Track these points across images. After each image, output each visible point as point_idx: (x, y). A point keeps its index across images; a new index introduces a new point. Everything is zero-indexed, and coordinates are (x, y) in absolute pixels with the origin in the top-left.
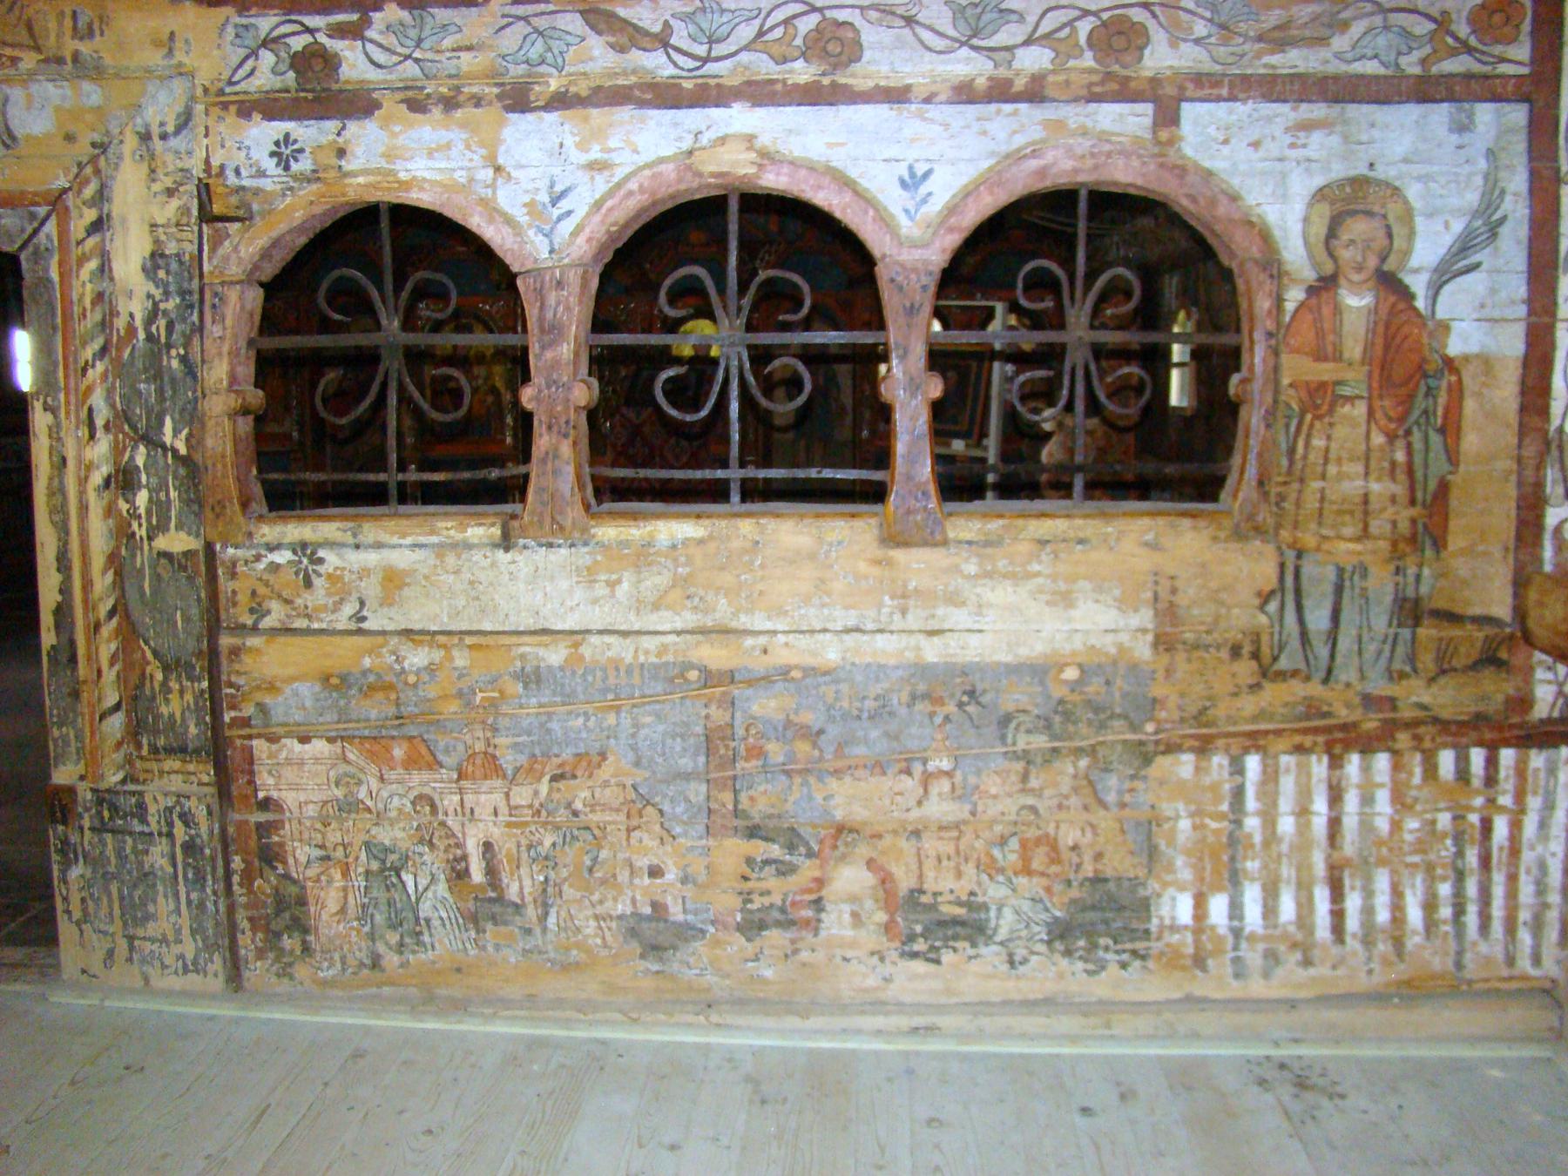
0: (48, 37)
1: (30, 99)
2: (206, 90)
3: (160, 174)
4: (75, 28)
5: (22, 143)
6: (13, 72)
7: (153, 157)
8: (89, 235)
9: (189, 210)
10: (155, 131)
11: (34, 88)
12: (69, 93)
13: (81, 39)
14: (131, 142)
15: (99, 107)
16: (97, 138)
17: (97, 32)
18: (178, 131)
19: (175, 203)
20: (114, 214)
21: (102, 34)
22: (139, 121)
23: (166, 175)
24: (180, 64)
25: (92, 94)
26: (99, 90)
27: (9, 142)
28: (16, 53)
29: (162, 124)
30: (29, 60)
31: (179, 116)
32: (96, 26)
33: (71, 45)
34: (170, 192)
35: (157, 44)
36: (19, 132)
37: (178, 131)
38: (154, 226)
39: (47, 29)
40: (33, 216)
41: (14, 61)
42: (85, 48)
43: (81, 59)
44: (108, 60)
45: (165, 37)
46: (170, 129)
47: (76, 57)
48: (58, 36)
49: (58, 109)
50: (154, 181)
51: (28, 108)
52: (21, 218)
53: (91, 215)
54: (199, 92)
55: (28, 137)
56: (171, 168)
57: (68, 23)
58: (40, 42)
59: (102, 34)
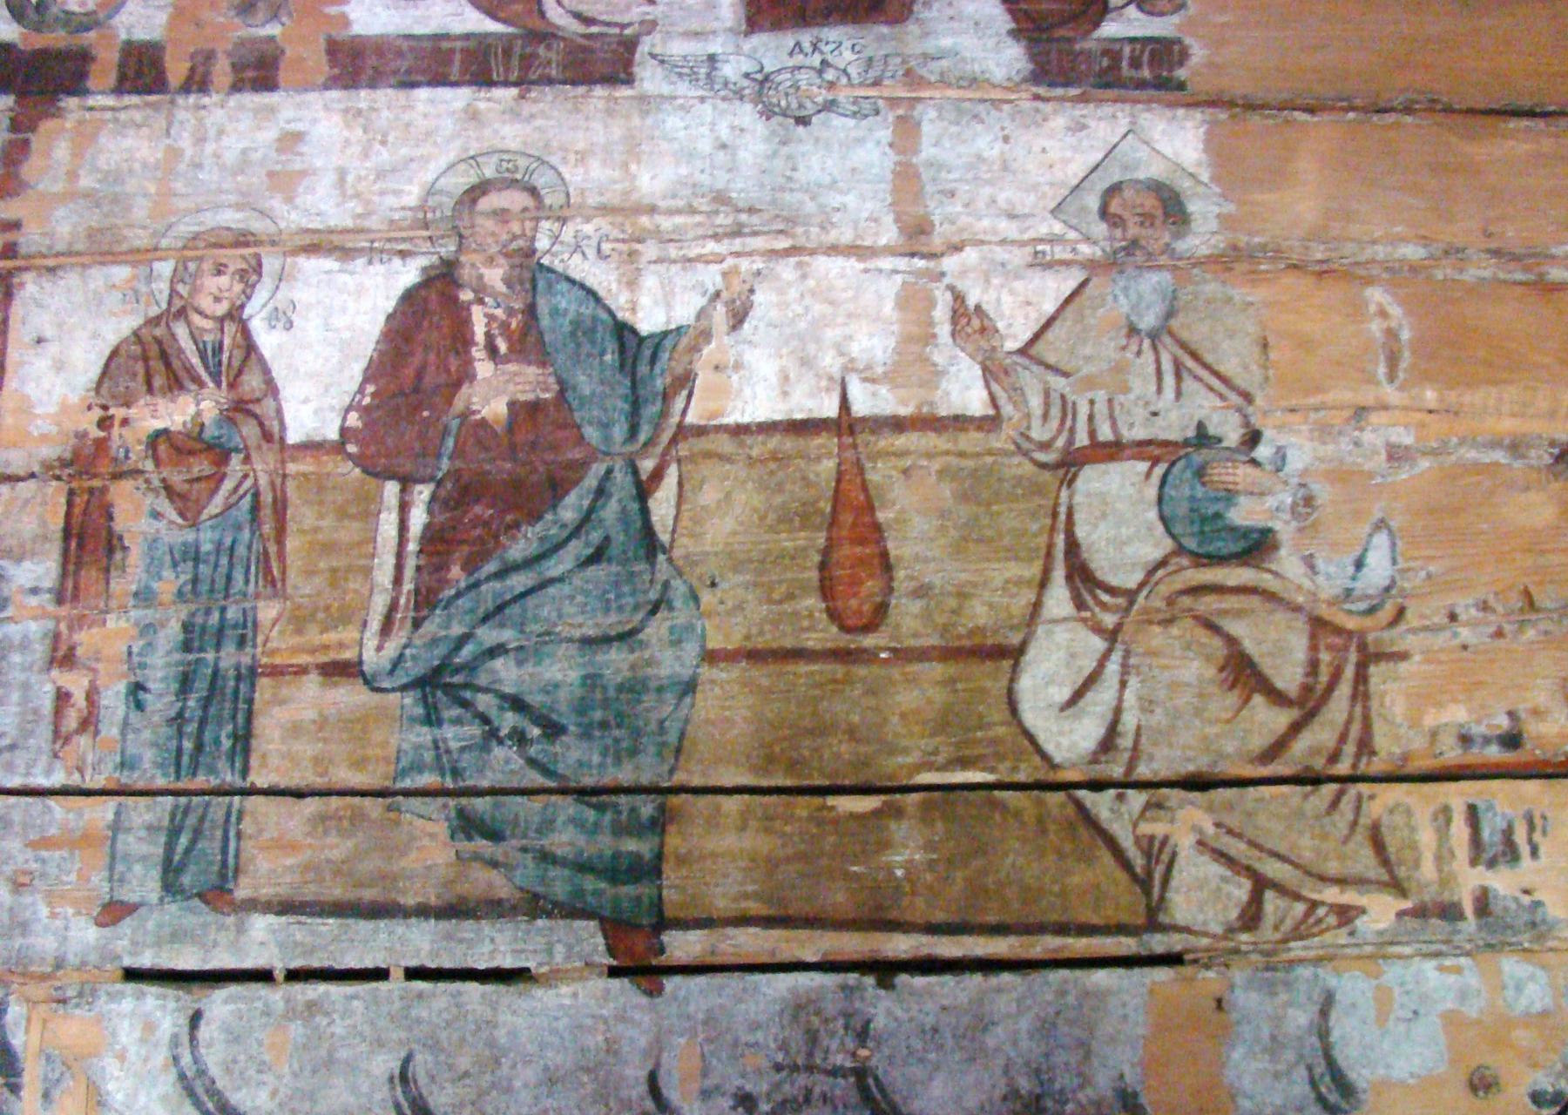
0: (1417, 864)
1: (1383, 999)
4: (1476, 842)
5: (1367, 1097)
6: (1342, 937)
11: (1393, 973)
12: (1472, 979)
13: (1492, 864)
15: (1544, 1013)
17: (1525, 850)
21: (1534, 852)
25: (1527, 984)
27: (1333, 1098)
28: (1350, 897)
30: (1380, 912)
32: (1520, 837)
33: (1469, 880)
36: (1359, 1076)
39: (1414, 846)
41: (1346, 915)
42: (1502, 882)
43: (1496, 907)
47: (1483, 903)
49: (1453, 1022)
51: (1382, 1017)
55: (1385, 1084)
57: (1460, 830)
58: (1402, 872)
59: (1534, 852)
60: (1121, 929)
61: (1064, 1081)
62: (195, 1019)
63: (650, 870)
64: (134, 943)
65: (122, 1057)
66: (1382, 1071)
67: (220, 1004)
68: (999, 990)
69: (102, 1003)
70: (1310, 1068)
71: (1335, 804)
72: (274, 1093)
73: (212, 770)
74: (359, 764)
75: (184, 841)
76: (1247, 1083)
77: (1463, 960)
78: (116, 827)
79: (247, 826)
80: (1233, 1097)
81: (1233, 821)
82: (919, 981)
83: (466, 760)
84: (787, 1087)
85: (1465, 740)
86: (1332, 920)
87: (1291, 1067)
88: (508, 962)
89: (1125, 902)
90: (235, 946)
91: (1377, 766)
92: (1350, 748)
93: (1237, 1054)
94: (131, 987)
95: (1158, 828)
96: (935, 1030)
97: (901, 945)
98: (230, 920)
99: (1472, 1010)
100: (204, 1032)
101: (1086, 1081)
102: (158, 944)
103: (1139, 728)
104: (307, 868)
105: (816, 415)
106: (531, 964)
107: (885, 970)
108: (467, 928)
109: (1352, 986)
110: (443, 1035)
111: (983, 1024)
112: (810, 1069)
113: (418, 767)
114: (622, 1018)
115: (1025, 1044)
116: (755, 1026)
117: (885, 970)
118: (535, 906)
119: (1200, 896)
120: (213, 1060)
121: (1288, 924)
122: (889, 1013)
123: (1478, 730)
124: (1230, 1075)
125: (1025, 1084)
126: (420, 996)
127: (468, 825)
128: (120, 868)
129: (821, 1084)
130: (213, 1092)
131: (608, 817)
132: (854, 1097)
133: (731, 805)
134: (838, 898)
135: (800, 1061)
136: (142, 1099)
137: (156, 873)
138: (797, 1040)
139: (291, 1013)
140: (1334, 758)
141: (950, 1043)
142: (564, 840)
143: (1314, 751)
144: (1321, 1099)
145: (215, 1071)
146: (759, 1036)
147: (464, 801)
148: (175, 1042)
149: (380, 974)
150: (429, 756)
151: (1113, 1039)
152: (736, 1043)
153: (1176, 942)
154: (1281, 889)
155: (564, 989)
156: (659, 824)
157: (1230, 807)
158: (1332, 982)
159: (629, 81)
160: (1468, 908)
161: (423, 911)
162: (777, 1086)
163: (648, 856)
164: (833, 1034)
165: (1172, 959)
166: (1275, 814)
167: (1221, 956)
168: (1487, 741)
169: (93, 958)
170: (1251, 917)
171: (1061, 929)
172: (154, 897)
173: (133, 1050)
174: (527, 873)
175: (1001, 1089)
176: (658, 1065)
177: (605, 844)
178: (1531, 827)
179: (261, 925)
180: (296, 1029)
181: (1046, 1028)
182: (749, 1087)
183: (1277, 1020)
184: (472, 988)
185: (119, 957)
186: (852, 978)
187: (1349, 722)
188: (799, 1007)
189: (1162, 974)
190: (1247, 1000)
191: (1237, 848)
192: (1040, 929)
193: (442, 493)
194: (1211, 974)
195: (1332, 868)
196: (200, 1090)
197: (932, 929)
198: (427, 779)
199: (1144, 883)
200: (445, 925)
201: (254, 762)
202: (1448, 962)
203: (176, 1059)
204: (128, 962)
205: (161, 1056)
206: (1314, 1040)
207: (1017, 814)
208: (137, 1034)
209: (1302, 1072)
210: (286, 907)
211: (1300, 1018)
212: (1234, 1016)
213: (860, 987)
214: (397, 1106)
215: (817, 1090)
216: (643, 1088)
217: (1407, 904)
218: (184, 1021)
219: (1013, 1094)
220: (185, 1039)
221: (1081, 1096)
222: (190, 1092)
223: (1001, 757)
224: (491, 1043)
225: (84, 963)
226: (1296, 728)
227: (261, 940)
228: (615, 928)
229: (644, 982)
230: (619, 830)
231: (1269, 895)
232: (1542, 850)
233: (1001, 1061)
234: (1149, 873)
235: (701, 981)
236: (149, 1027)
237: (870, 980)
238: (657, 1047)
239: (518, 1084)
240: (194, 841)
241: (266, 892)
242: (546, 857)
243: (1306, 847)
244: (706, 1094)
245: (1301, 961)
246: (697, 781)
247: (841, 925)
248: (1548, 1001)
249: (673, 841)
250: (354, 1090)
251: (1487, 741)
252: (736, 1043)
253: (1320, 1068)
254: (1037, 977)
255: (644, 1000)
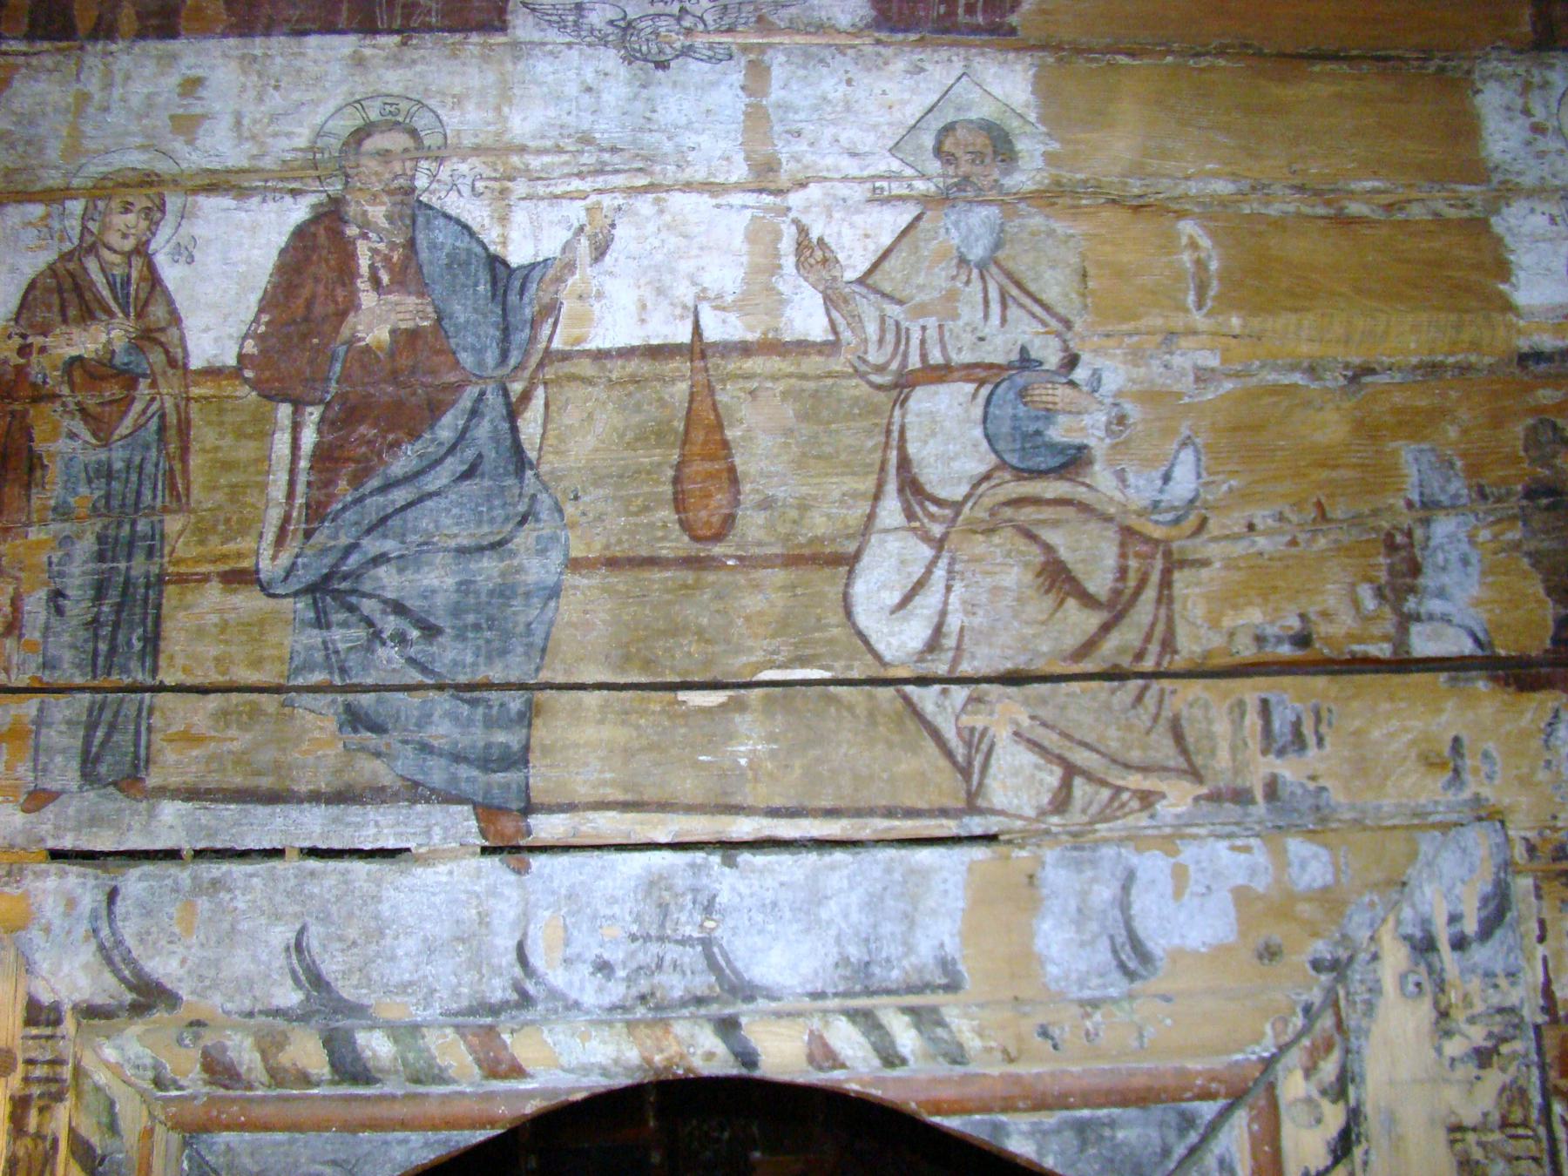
0: (1213, 752)
1: (1180, 875)
2: (1531, 849)
3: (1459, 1016)
5: (1163, 965)
6: (1143, 820)
7: (1441, 986)
8: (1336, 1161)
9: (1523, 1092)
10: (1443, 938)
11: (1188, 853)
12: (1260, 857)
13: (1281, 753)
14: (1395, 957)
15: (1325, 889)
16: (1321, 948)
17: (1311, 740)
18: (1485, 933)
19: (1494, 1079)
20: (1368, 1109)
21: (1320, 742)
22: (1407, 913)
23: (1472, 1020)
24: (1477, 800)
26: (1324, 855)
27: (1132, 964)
29: (1454, 919)
30: (1177, 799)
31: (1485, 901)
32: (1307, 730)
33: (1263, 767)
34: (1483, 1057)
35: (1431, 762)
36: (1157, 945)
37: (1485, 933)
38: (1457, 1128)
39: (1210, 736)
40: (1187, 1121)
41: (1147, 799)
42: (1288, 770)
43: (1284, 793)
44: (1337, 795)
45: (1446, 750)
46: (1470, 927)
47: (1272, 789)
48: (1234, 750)
49: (1242, 896)
50: (1448, 1034)
51: (1178, 893)
52: (1162, 1124)
53: (1334, 1117)
54: (1519, 852)
55: (1177, 954)
56: (1479, 1007)
57: (1252, 720)
58: (1199, 761)
59: (1320, 742)
60: (944, 812)
61: (892, 950)
62: (112, 895)
63: (519, 759)
64: (57, 827)
65: (47, 930)
66: (1177, 941)
67: (135, 882)
68: (833, 868)
69: (30, 883)
70: (1112, 938)
71: (1139, 699)
72: (183, 962)
73: (125, 670)
74: (257, 663)
75: (100, 734)
76: (1054, 951)
77: (1253, 841)
78: (40, 721)
79: (156, 720)
80: (1042, 964)
81: (1045, 713)
82: (760, 859)
83: (353, 661)
84: (641, 956)
85: (1260, 640)
86: (1135, 804)
87: (1095, 937)
88: (391, 844)
89: (945, 786)
90: (146, 830)
91: (1179, 662)
92: (1154, 648)
93: (1046, 926)
94: (54, 867)
95: (979, 722)
96: (774, 904)
97: (744, 828)
98: (144, 804)
99: (1261, 885)
100: (120, 907)
101: (910, 949)
102: (78, 829)
103: (962, 629)
104: (210, 759)
105: (671, 340)
106: (412, 845)
107: (728, 847)
108: (354, 812)
109: (1153, 866)
110: (334, 909)
111: (818, 899)
112: (661, 939)
113: (307, 667)
114: (492, 892)
115: (855, 917)
116: (612, 901)
117: (728, 847)
118: (415, 792)
119: (1016, 783)
120: (129, 932)
121: (1094, 809)
122: (733, 889)
123: (1271, 631)
124: (1039, 944)
125: (855, 952)
126: (312, 874)
127: (355, 719)
128: (43, 759)
129: (672, 952)
130: (130, 961)
131: (481, 710)
132: (701, 964)
133: (592, 699)
134: (687, 786)
135: (653, 932)
136: (66, 969)
137: (75, 764)
138: (650, 912)
139: (198, 888)
140: (1140, 656)
141: (788, 915)
142: (441, 731)
143: (1121, 651)
144: (1122, 966)
145: (130, 942)
146: (616, 909)
147: (350, 697)
148: (94, 916)
149: (277, 853)
150: (319, 656)
151: (934, 912)
152: (595, 917)
153: (991, 824)
154: (1089, 776)
155: (442, 868)
156: (527, 717)
157: (1043, 701)
158: (1134, 860)
159: (503, 28)
160: (1259, 795)
161: (316, 797)
162: (633, 954)
163: (516, 747)
164: (682, 908)
165: (990, 839)
166: (1082, 706)
167: (1035, 836)
168: (1279, 640)
169: (20, 840)
170: (1061, 802)
171: (889, 813)
172: (74, 786)
173: (57, 922)
174: (407, 763)
175: (834, 955)
176: (525, 934)
177: (478, 737)
178: (1318, 720)
179: (170, 810)
180: (203, 904)
181: (873, 903)
182: (606, 956)
183: (1084, 895)
184: (359, 867)
185: (43, 840)
186: (699, 856)
187: (1153, 625)
188: (653, 884)
189: (979, 853)
190: (1057, 875)
191: (1050, 739)
192: (871, 812)
193: (331, 415)
194: (1024, 853)
195: (1135, 756)
196: (117, 959)
197: (774, 813)
198: (317, 677)
199: (966, 772)
200: (335, 810)
201: (163, 662)
202: (1239, 842)
203: (95, 931)
204: (51, 844)
205: (83, 927)
206: (1117, 913)
207: (851, 708)
208: (61, 909)
209: (1104, 945)
210: (192, 794)
211: (1104, 893)
212: (1045, 891)
213: (706, 866)
214: (293, 972)
215: (668, 958)
216: (512, 956)
217: (1204, 790)
218: (103, 897)
219: (845, 961)
220: (104, 913)
221: (905, 963)
222: (110, 961)
223: (837, 657)
224: (376, 917)
225: (12, 846)
226: (1106, 628)
227: (171, 823)
228: (487, 812)
229: (513, 859)
230: (489, 723)
231: (1078, 781)
232: (1328, 740)
233: (833, 932)
234: (970, 762)
235: (564, 860)
236: (71, 903)
237: (715, 859)
238: (525, 918)
239: (400, 952)
240: (108, 735)
241: (174, 780)
242: (425, 748)
243: (1113, 739)
244: (568, 962)
245: (1106, 841)
246: (560, 679)
247: (690, 809)
248: (1329, 878)
249: (541, 733)
250: (255, 959)
251: (1279, 640)
252: (595, 917)
253: (1121, 938)
254: (866, 856)
255: (512, 877)
